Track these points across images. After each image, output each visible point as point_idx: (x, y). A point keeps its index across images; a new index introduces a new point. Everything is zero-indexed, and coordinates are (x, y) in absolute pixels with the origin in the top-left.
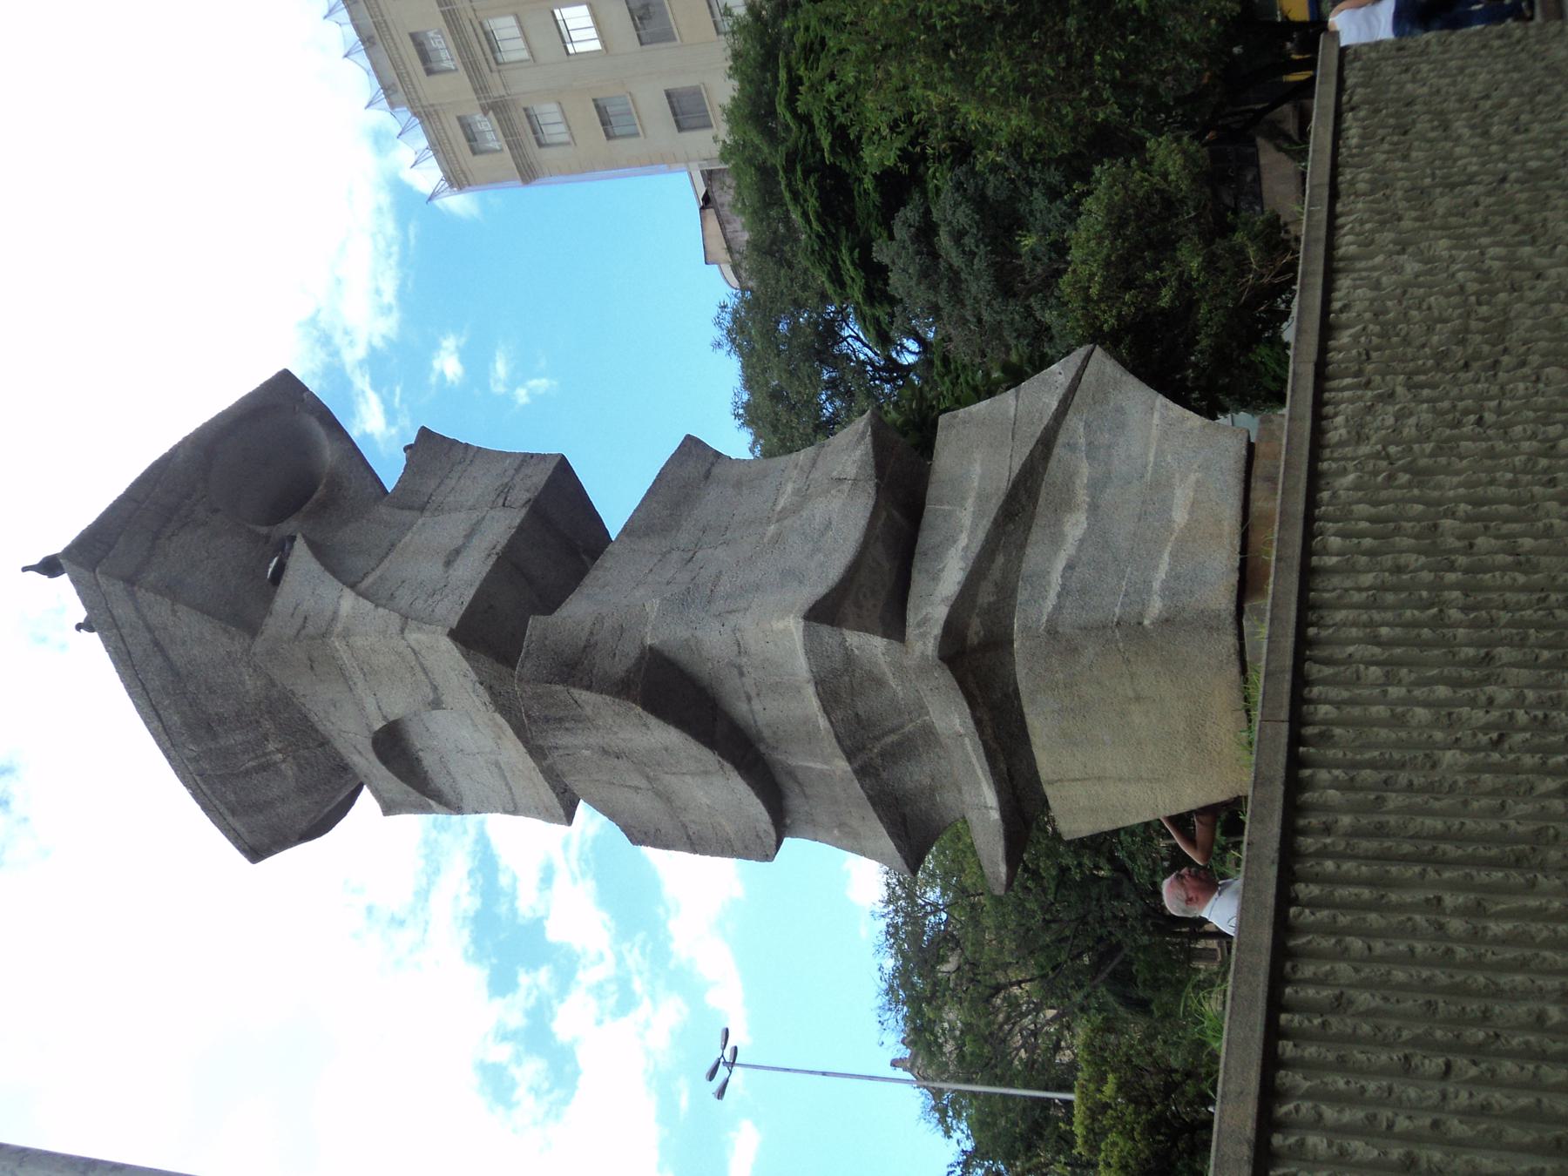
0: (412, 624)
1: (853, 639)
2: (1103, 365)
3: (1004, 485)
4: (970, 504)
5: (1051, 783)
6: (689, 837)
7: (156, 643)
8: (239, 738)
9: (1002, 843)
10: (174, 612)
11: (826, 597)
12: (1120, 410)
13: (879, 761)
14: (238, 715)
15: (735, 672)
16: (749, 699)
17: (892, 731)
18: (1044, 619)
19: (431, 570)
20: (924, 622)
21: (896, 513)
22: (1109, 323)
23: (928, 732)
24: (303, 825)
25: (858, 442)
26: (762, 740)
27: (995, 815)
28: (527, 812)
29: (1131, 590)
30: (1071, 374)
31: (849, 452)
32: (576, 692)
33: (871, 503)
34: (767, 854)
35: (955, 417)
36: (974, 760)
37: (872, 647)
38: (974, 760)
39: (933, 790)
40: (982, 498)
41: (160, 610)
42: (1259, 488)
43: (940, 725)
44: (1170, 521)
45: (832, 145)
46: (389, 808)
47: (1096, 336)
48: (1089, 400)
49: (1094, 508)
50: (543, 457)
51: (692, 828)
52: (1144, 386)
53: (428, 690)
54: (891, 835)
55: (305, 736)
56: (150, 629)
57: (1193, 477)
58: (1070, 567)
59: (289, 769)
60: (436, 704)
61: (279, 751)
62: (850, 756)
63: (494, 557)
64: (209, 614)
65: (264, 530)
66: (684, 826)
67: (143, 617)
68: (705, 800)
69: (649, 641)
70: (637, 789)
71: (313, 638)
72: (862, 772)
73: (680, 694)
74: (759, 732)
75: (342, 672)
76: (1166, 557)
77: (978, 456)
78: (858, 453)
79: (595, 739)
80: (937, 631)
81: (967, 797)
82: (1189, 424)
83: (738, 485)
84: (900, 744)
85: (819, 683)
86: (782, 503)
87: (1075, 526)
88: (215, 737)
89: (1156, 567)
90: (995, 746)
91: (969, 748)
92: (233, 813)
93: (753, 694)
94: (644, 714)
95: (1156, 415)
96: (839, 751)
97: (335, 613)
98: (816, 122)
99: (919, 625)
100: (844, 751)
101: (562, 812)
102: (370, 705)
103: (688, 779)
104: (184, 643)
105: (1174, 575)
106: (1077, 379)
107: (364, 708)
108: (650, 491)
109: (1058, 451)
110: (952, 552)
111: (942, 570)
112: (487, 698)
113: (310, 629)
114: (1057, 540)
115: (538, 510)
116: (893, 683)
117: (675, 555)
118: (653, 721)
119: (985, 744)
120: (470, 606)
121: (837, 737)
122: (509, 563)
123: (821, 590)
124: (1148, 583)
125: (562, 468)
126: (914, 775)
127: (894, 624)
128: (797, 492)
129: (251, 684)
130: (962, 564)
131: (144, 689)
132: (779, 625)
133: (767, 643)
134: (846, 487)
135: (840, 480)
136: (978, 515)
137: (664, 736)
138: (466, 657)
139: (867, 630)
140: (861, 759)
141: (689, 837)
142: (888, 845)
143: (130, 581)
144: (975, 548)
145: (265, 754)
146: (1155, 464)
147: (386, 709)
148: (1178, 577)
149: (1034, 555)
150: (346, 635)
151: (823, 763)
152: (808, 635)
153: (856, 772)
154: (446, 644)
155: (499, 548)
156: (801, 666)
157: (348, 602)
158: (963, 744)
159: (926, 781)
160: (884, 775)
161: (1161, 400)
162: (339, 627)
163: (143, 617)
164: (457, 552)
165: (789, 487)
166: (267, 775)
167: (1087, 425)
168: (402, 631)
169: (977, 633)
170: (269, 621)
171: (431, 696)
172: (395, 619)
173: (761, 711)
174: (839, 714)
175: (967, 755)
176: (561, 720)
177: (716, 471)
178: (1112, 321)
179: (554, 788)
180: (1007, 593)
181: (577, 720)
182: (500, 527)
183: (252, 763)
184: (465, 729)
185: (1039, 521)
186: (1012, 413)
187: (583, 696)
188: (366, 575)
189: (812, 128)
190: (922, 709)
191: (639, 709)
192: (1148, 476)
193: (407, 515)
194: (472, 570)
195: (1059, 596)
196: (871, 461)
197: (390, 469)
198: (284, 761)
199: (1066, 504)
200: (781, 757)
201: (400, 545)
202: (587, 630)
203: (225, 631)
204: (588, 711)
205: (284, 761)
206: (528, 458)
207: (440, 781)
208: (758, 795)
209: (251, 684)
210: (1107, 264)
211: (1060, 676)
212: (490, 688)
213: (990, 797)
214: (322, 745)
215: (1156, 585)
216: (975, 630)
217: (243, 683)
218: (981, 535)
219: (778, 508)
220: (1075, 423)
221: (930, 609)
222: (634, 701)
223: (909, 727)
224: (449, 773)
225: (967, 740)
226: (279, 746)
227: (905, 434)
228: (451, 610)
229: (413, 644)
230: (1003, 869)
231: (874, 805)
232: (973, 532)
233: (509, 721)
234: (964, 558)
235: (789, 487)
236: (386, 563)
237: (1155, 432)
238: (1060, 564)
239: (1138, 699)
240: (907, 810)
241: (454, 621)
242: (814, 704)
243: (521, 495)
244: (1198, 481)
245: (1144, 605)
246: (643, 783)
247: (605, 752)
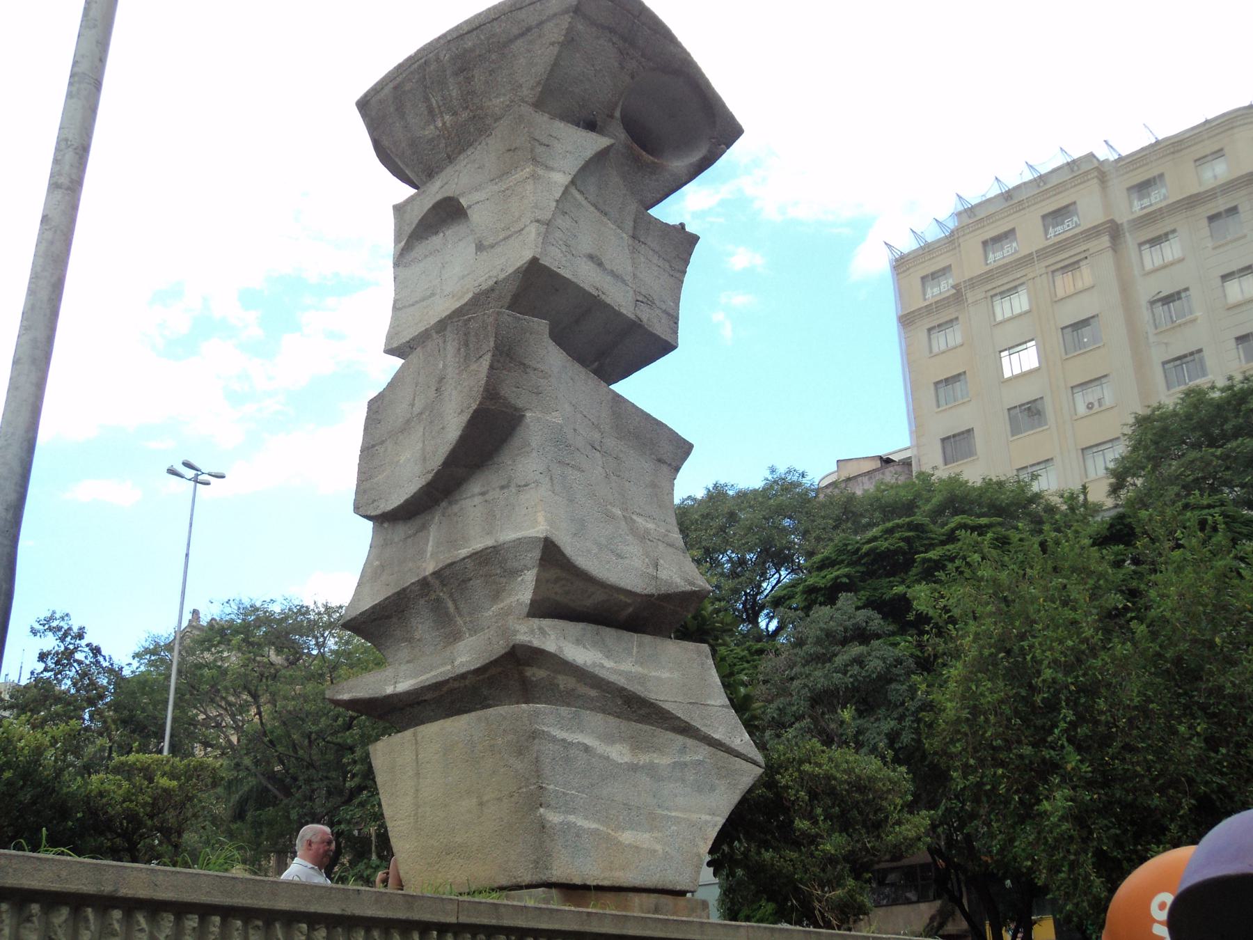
0: (543, 229)
1: (530, 577)
2: (748, 775)
3: (652, 696)
4: (638, 669)
5: (415, 735)
6: (373, 446)
7: (529, 29)
8: (454, 94)
9: (367, 696)
10: (553, 44)
11: (563, 555)
12: (713, 789)
13: (433, 597)
14: (474, 92)
15: (504, 483)
16: (483, 494)
17: (457, 608)
19: (586, 243)
20: (542, 631)
21: (631, 609)
22: (783, 780)
23: (455, 637)
24: (386, 143)
25: (686, 580)
26: (450, 503)
27: (389, 690)
28: (394, 318)
29: (568, 798)
31: (679, 572)
32: (488, 357)
33: (638, 590)
34: (357, 509)
35: (707, 657)
36: (433, 673)
37: (524, 591)
38: (433, 673)
39: (410, 640)
40: (642, 679)
41: (555, 32)
43: (461, 645)
45: (930, 560)
46: (399, 209)
47: (772, 769)
48: (720, 764)
49: (634, 768)
50: (676, 332)
51: (381, 449)
52: (732, 807)
53: (491, 240)
54: (374, 607)
55: (458, 143)
56: (541, 23)
57: (658, 847)
58: (587, 749)
59: (430, 131)
60: (480, 247)
61: (444, 124)
62: (436, 574)
64: (552, 70)
65: (617, 114)
66: (382, 442)
67: (549, 19)
68: (403, 459)
69: (528, 414)
70: (413, 405)
71: (532, 150)
72: (424, 583)
73: (487, 437)
74: (456, 502)
75: (504, 174)
76: (594, 826)
77: (676, 675)
78: (678, 580)
79: (451, 372)
80: (536, 643)
81: (404, 667)
82: (701, 844)
83: (653, 485)
84: (447, 614)
85: (495, 549)
86: (639, 520)
87: (619, 753)
88: (456, 74)
89: (586, 818)
90: (445, 689)
91: (442, 669)
92: (395, 88)
93: (487, 497)
94: (471, 411)
95: (708, 818)
96: (440, 566)
97: (552, 169)
98: (947, 547)
99: (540, 629)
100: (442, 569)
101: (395, 345)
102: (477, 196)
103: (420, 445)
104: (529, 51)
105: (579, 833)
106: (738, 755)
107: (477, 190)
108: (648, 416)
109: (680, 739)
110: (600, 655)
111: (584, 647)
112: (484, 287)
113: (540, 150)
114: (609, 739)
115: (634, 327)
117: (597, 436)
118: (465, 417)
119: (447, 682)
120: (557, 275)
121: (452, 564)
122: (591, 305)
123: (568, 550)
124: (573, 811)
125: (665, 347)
126: (422, 626)
127: (543, 609)
128: (647, 531)
129: (496, 103)
130: (589, 662)
131: (494, 20)
132: (541, 518)
133: (526, 508)
134: (651, 570)
135: (656, 566)
136: (628, 676)
137: (453, 427)
138: (517, 271)
139: (537, 587)
140: (435, 583)
141: (373, 446)
142: (366, 604)
143: (577, 10)
144: (603, 674)
145: (441, 113)
146: (669, 817)
147: (476, 207)
149: (596, 720)
150: (534, 176)
151: (432, 552)
152: (532, 541)
153: (425, 578)
154: (527, 255)
155: (603, 297)
156: (508, 535)
157: (560, 179)
158: (443, 665)
160: (422, 602)
161: (720, 821)
162: (540, 172)
163: (549, 19)
164: (600, 264)
165: (651, 526)
166: (425, 117)
167: (700, 763)
168: (538, 221)
169: (534, 675)
170: (546, 117)
171: (486, 243)
172: (547, 215)
173: (473, 503)
174: (470, 564)
176: (466, 345)
177: (665, 468)
178: (783, 782)
179: (413, 339)
180: (567, 698)
181: (467, 358)
182: (620, 299)
183: (433, 101)
184: (462, 269)
185: (624, 725)
187: (485, 363)
188: (581, 192)
189: (943, 543)
190: (474, 631)
191: (474, 406)
193: (629, 224)
194: (585, 276)
195: (564, 740)
196: (671, 591)
197: (669, 211)
198: (436, 127)
199: (637, 745)
201: (605, 220)
202: (539, 366)
203: (539, 83)
204: (474, 367)
205: (436, 127)
206: (674, 319)
207: (420, 249)
208: (407, 501)
209: (496, 103)
210: (829, 777)
211: (500, 741)
212: (492, 289)
213: (404, 686)
214: (449, 157)
215: (572, 818)
216: (537, 673)
218: (613, 678)
219: (634, 517)
220: (701, 753)
221: (553, 637)
222: (481, 403)
223: (460, 621)
224: (426, 256)
225: (449, 667)
226: (448, 125)
227: (694, 618)
228: (555, 260)
229: (527, 229)
230: (346, 697)
231: (398, 593)
232: (615, 671)
233: (466, 304)
234: (594, 664)
235: (651, 526)
236: (592, 209)
237: (694, 817)
239: (481, 804)
240: (394, 620)
241: (545, 261)
242: (479, 546)
243: (646, 315)
244: (655, 851)
245: (555, 809)
246: (417, 410)
247: (441, 380)
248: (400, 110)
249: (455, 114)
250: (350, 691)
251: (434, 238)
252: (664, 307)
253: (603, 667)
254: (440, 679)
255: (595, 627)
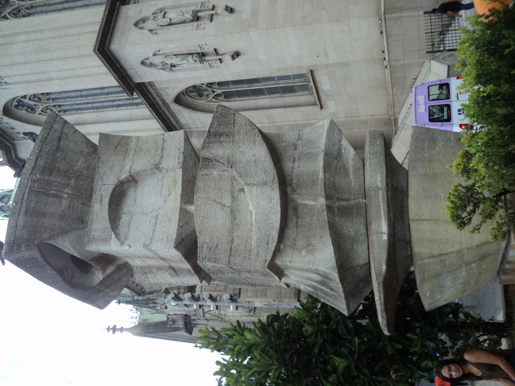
13: (336, 210)
14: (67, 171)
15: (293, 147)
16: (294, 161)
26: (291, 185)
27: (385, 237)
36: (381, 204)
38: (381, 204)
53: (158, 158)
59: (65, 203)
61: (68, 194)
62: (328, 197)
91: (381, 197)
93: (297, 158)
96: (323, 193)
100: (325, 192)
116: (352, 176)
119: (388, 202)
156: (322, 142)
158: (378, 195)
159: (353, 234)
175: (379, 202)
183: (54, 192)
198: (66, 199)
200: (295, 197)
205: (66, 199)
207: (122, 230)
211: (427, 155)
212: (185, 157)
213: (384, 227)
214: (83, 204)
217: (78, 162)
223: (352, 202)
225: (381, 192)
226: (69, 192)
233: (183, 175)
242: (321, 164)
248: (41, 215)
249: (68, 185)
250: (382, 265)
251: (122, 220)
254: (385, 200)
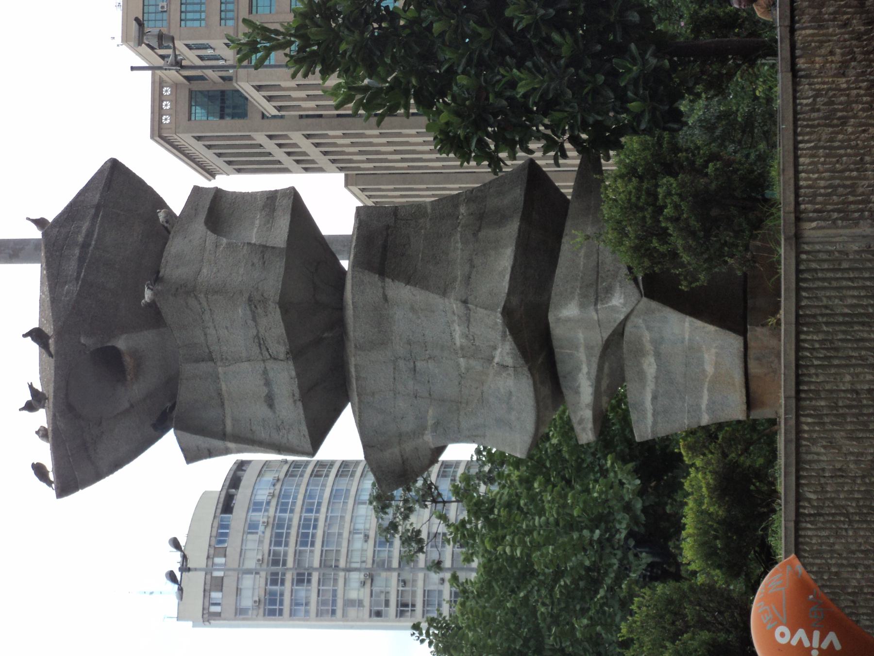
4: (582, 349)
18: (649, 430)
19: (261, 410)
20: (581, 422)
25: (504, 340)
30: (629, 310)
33: (531, 382)
40: (589, 348)
42: (752, 364)
44: (704, 371)
49: (658, 355)
52: (676, 312)
57: (713, 351)
58: (655, 398)
63: (299, 404)
69: (433, 446)
87: (650, 366)
89: (702, 397)
105: (712, 402)
110: (580, 375)
111: (579, 387)
114: (641, 375)
117: (401, 363)
124: (698, 406)
130: (589, 383)
146: (690, 340)
148: (714, 403)
155: (297, 395)
186: (596, 317)
192: (687, 342)
193: (205, 367)
195: (653, 415)
199: (639, 352)
215: (704, 407)
218: (595, 366)
234: (589, 379)
236: (226, 405)
238: (649, 397)
244: (717, 353)
252: (251, 323)
253: (588, 373)
255: (561, 380)
